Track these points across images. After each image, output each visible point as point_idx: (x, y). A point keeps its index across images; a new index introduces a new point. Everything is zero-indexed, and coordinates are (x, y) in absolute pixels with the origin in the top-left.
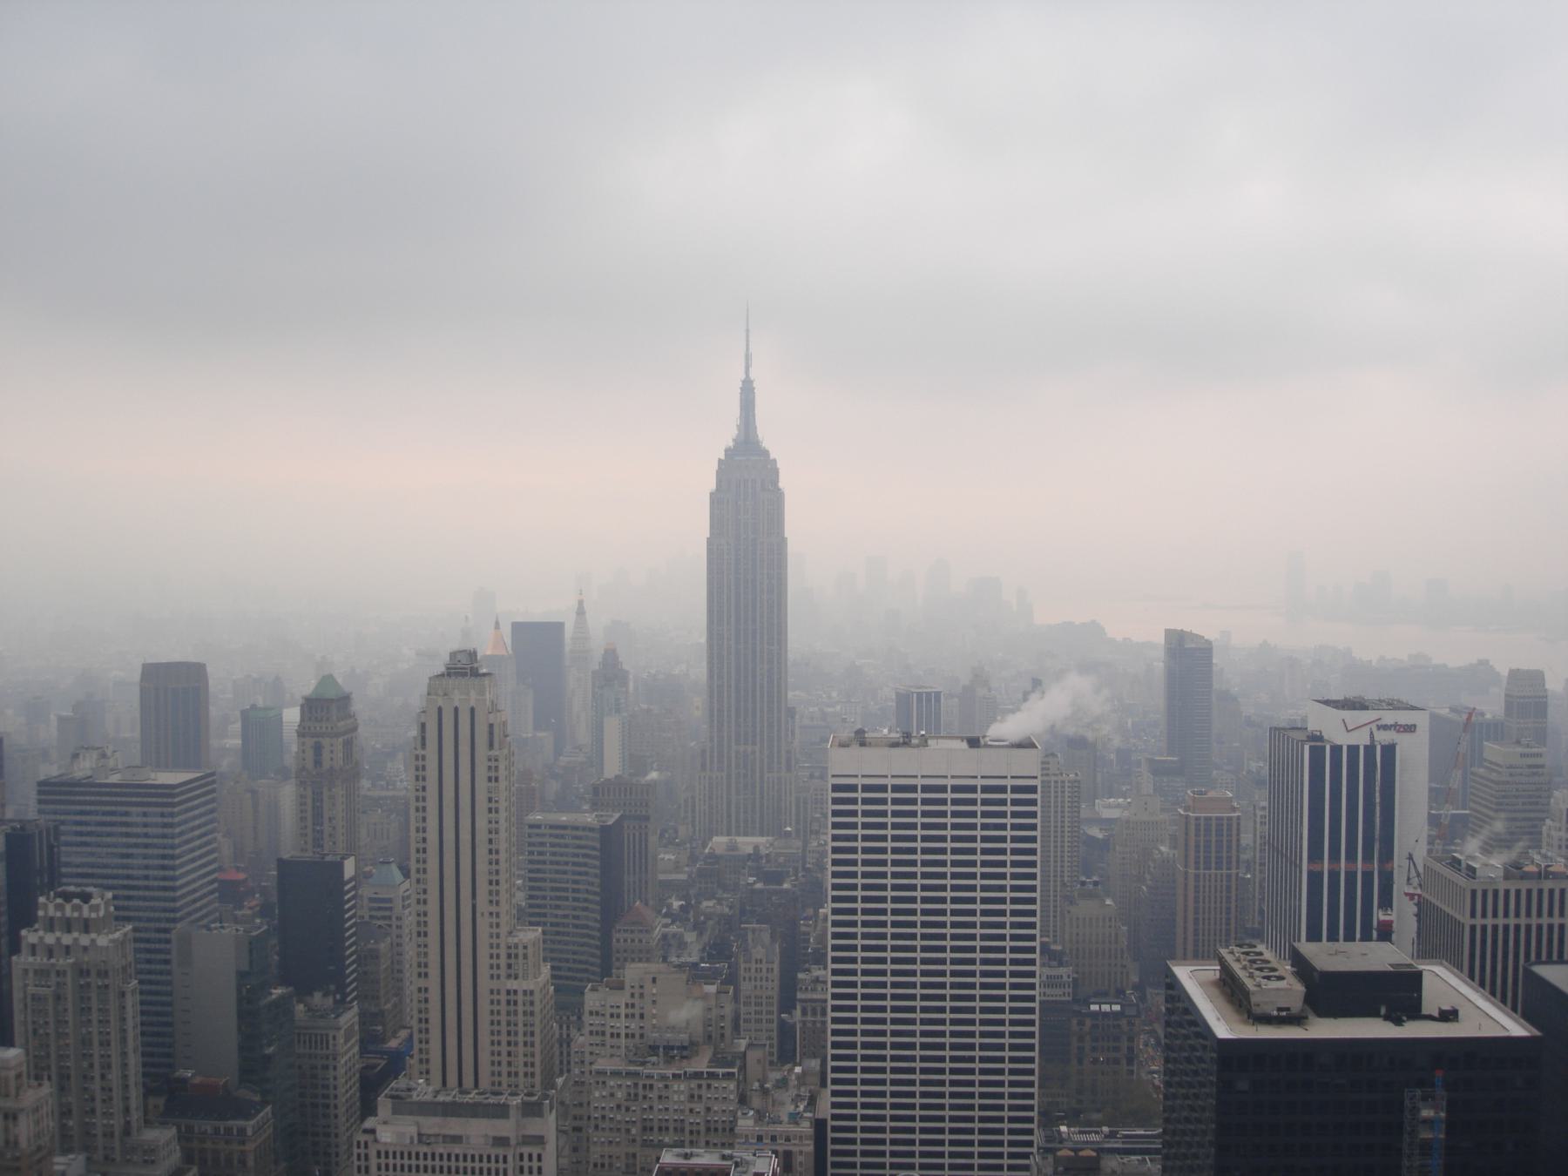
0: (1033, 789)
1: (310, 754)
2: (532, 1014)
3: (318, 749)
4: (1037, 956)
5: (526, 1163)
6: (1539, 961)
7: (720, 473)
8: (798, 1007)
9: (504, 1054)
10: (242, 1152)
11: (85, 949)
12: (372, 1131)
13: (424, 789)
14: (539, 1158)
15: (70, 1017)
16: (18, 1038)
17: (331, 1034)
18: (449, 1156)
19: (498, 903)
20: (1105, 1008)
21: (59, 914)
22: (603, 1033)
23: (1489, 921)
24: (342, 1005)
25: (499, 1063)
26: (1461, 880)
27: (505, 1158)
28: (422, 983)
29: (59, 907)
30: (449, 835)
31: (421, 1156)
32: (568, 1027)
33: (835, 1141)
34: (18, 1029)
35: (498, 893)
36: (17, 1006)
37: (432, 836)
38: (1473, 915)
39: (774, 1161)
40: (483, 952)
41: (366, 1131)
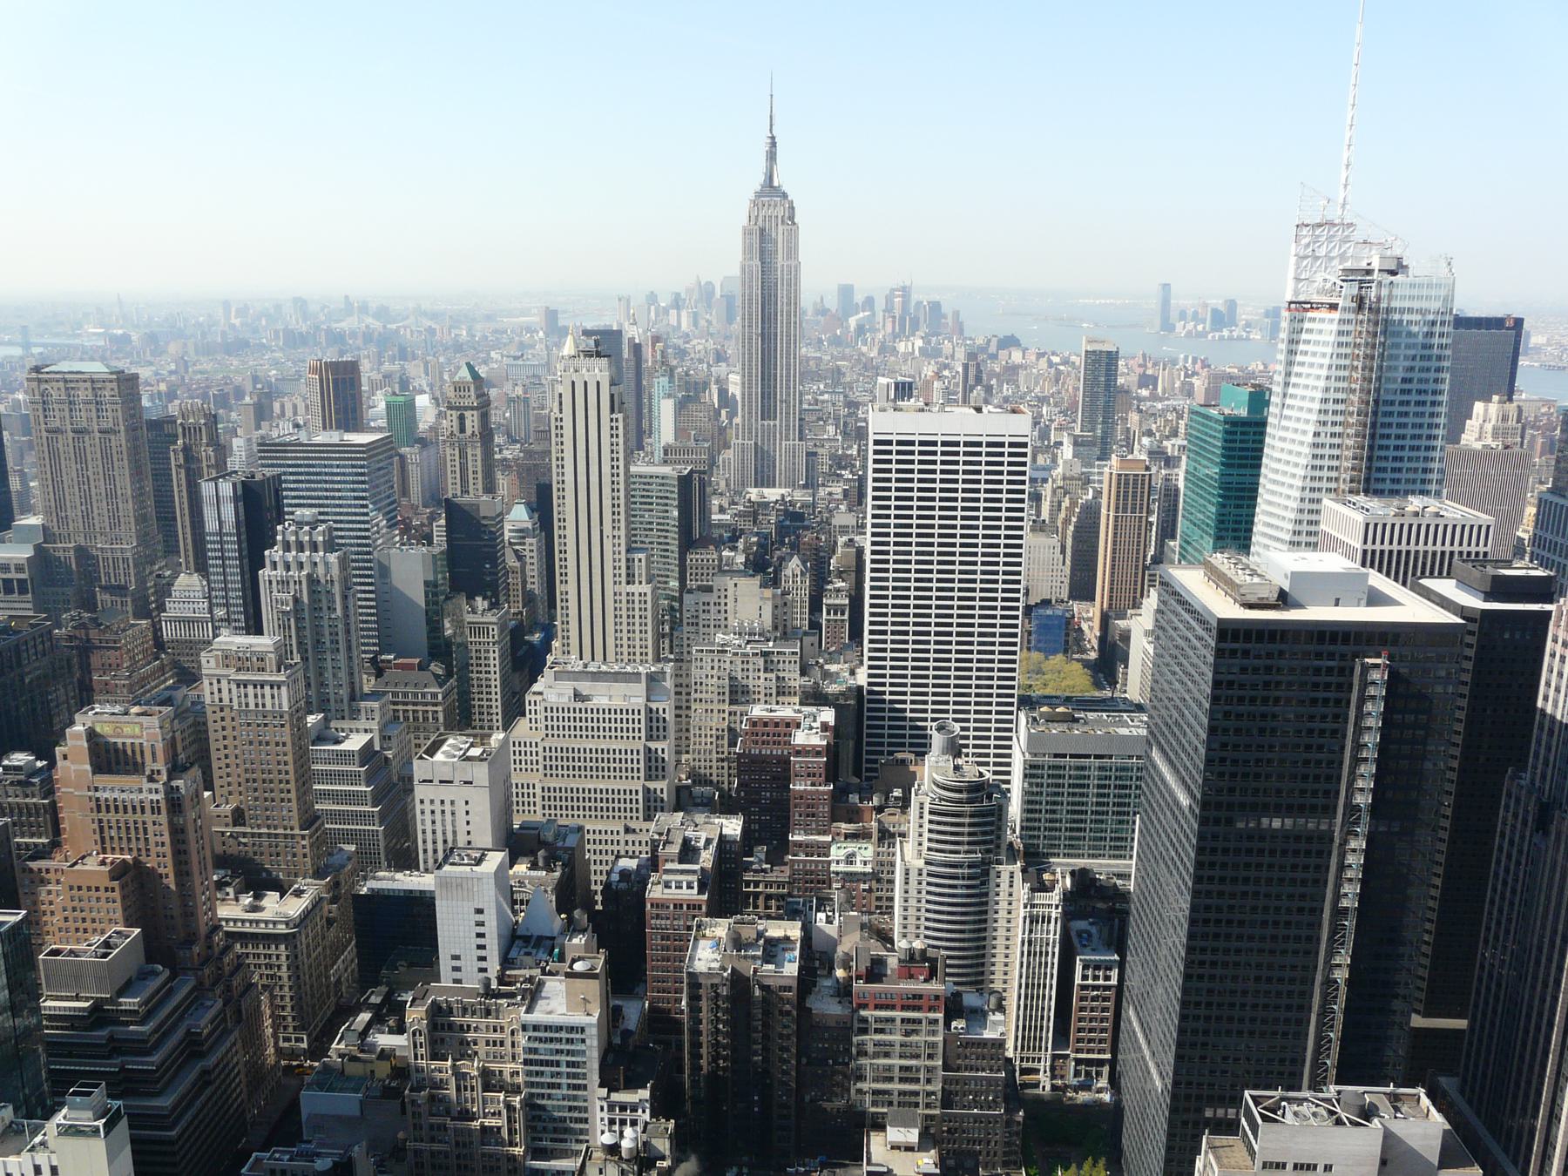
1: (456, 423)
2: (646, 610)
3: (462, 418)
6: (1423, 575)
12: (540, 693)
15: (306, 615)
22: (697, 624)
37: (569, 478)
41: (534, 693)
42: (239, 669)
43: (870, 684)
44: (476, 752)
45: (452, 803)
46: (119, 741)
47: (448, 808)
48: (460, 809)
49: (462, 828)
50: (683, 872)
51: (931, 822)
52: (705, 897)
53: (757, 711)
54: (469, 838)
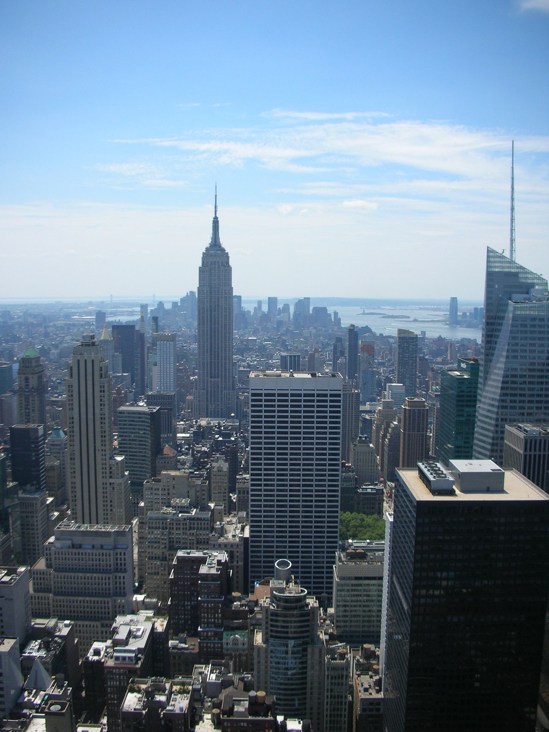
0: (339, 396)
3: (27, 379)
4: (340, 467)
5: (119, 556)
7: (203, 258)
8: (237, 491)
9: (109, 510)
12: (52, 543)
13: (72, 395)
14: (124, 555)
17: (35, 502)
18: (86, 553)
19: (105, 445)
20: (369, 491)
23: (533, 453)
25: (107, 514)
26: (522, 435)
27: (110, 554)
28: (73, 480)
30: (83, 416)
31: (74, 554)
32: (137, 500)
33: (252, 547)
35: (105, 441)
37: (76, 416)
38: (526, 450)
39: (226, 555)
40: (99, 467)
41: (49, 543)
43: (251, 536)
50: (125, 651)
51: (272, 620)
52: (139, 666)
53: (180, 553)
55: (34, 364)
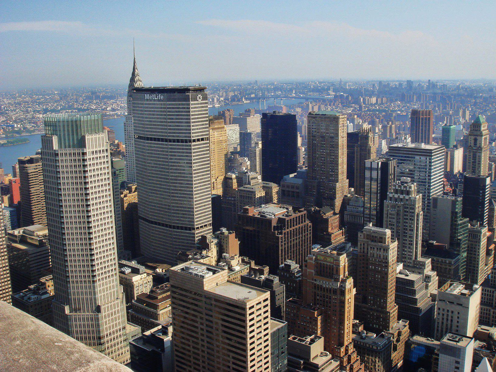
1: (473, 142)
3: (476, 140)
10: (450, 269)
11: (407, 200)
16: (384, 226)
17: (479, 234)
21: (399, 189)
24: (482, 225)
29: (400, 186)
34: (384, 223)
36: (385, 216)
42: (372, 241)
44: (466, 292)
45: (452, 312)
46: (325, 263)
47: (450, 313)
48: (455, 316)
49: (455, 323)
54: (456, 328)
55: (482, 129)
